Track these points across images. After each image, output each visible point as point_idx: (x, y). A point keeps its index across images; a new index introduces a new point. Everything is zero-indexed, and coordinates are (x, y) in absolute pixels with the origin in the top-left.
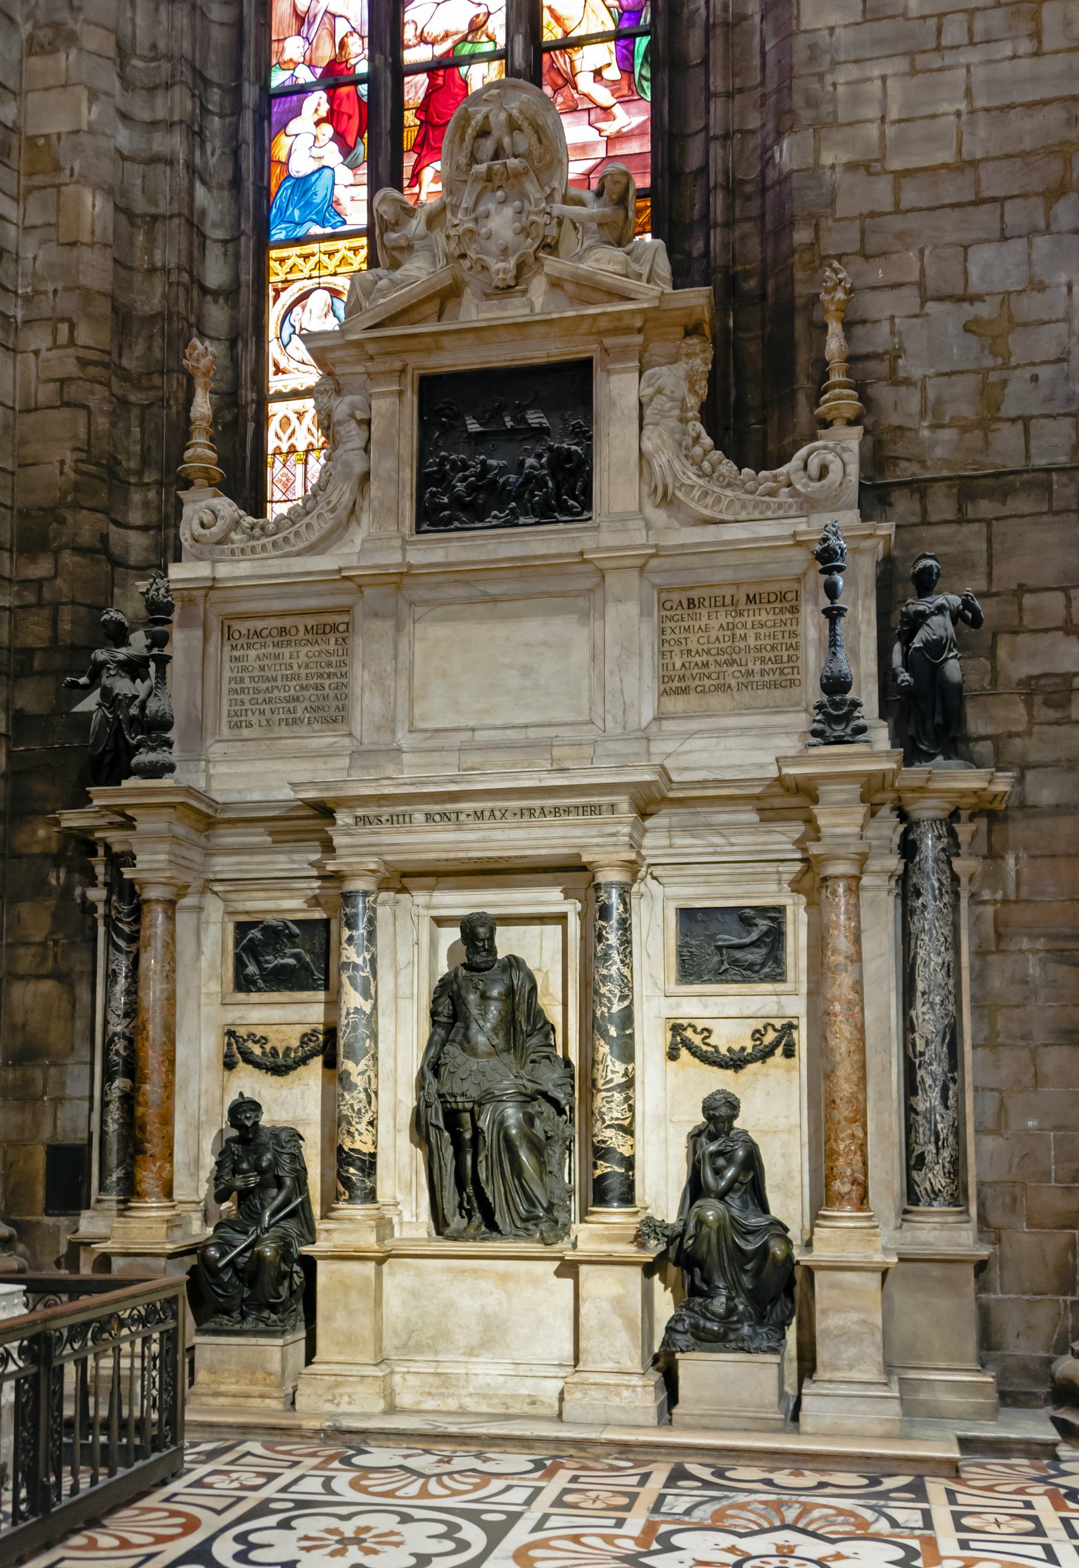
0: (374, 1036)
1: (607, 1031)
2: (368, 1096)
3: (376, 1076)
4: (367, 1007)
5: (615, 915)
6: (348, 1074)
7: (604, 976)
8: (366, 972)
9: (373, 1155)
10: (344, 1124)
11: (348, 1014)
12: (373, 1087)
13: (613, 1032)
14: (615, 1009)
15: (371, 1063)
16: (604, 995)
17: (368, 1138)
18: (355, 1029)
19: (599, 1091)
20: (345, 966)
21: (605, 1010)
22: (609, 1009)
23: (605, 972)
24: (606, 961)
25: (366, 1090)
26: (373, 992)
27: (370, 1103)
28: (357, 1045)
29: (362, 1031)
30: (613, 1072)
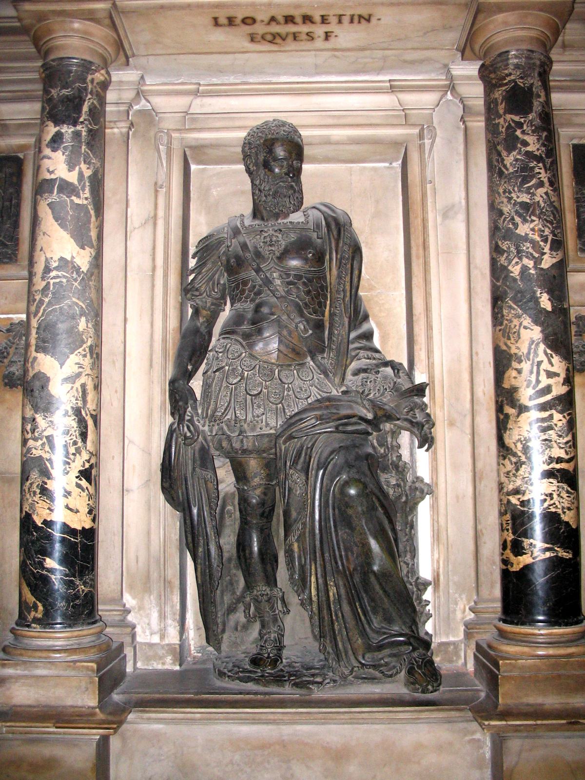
0: (96, 315)
1: (537, 301)
2: (82, 422)
3: (97, 387)
4: (83, 259)
5: (537, 106)
6: (43, 380)
7: (525, 206)
8: (84, 199)
9: (90, 534)
10: (34, 475)
11: (47, 270)
12: (91, 406)
13: (546, 303)
14: (547, 262)
15: (87, 362)
16: (525, 238)
17: (81, 502)
18: (57, 297)
19: (522, 409)
20: (42, 187)
21: (530, 264)
22: (538, 261)
23: (525, 198)
24: (525, 180)
25: (77, 412)
26: (93, 234)
27: (84, 436)
28: (62, 327)
29: (73, 302)
30: (550, 375)
